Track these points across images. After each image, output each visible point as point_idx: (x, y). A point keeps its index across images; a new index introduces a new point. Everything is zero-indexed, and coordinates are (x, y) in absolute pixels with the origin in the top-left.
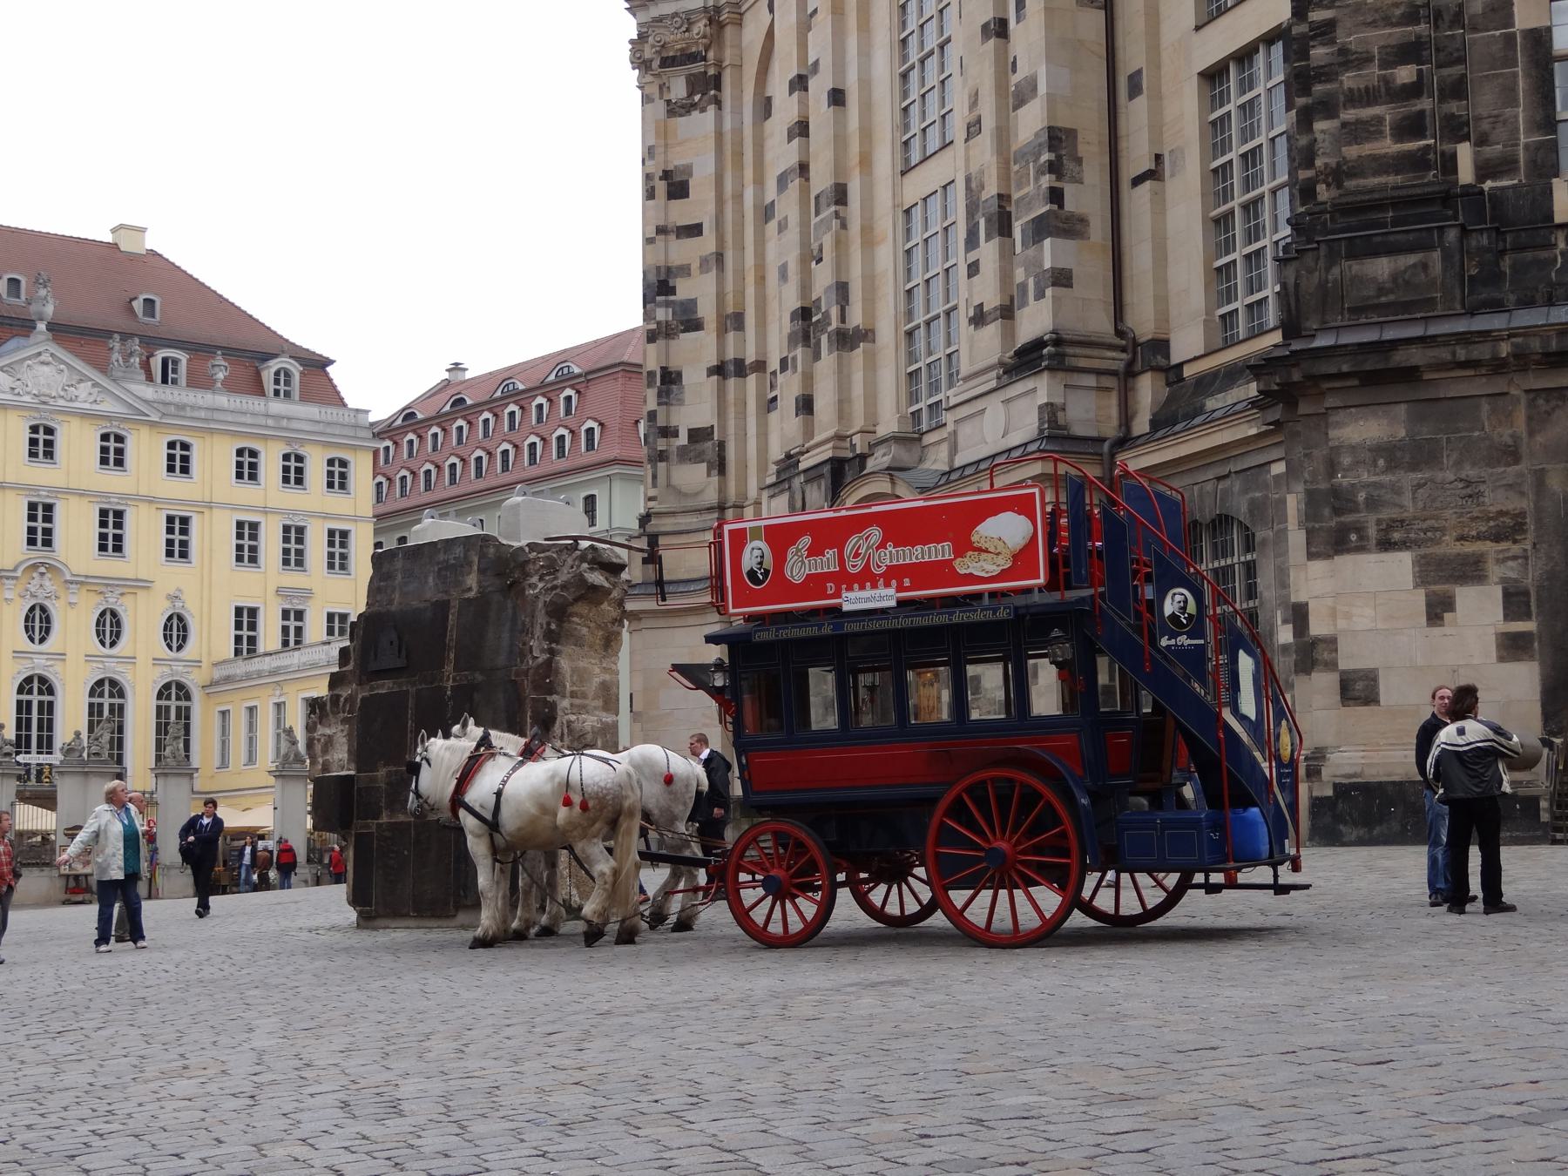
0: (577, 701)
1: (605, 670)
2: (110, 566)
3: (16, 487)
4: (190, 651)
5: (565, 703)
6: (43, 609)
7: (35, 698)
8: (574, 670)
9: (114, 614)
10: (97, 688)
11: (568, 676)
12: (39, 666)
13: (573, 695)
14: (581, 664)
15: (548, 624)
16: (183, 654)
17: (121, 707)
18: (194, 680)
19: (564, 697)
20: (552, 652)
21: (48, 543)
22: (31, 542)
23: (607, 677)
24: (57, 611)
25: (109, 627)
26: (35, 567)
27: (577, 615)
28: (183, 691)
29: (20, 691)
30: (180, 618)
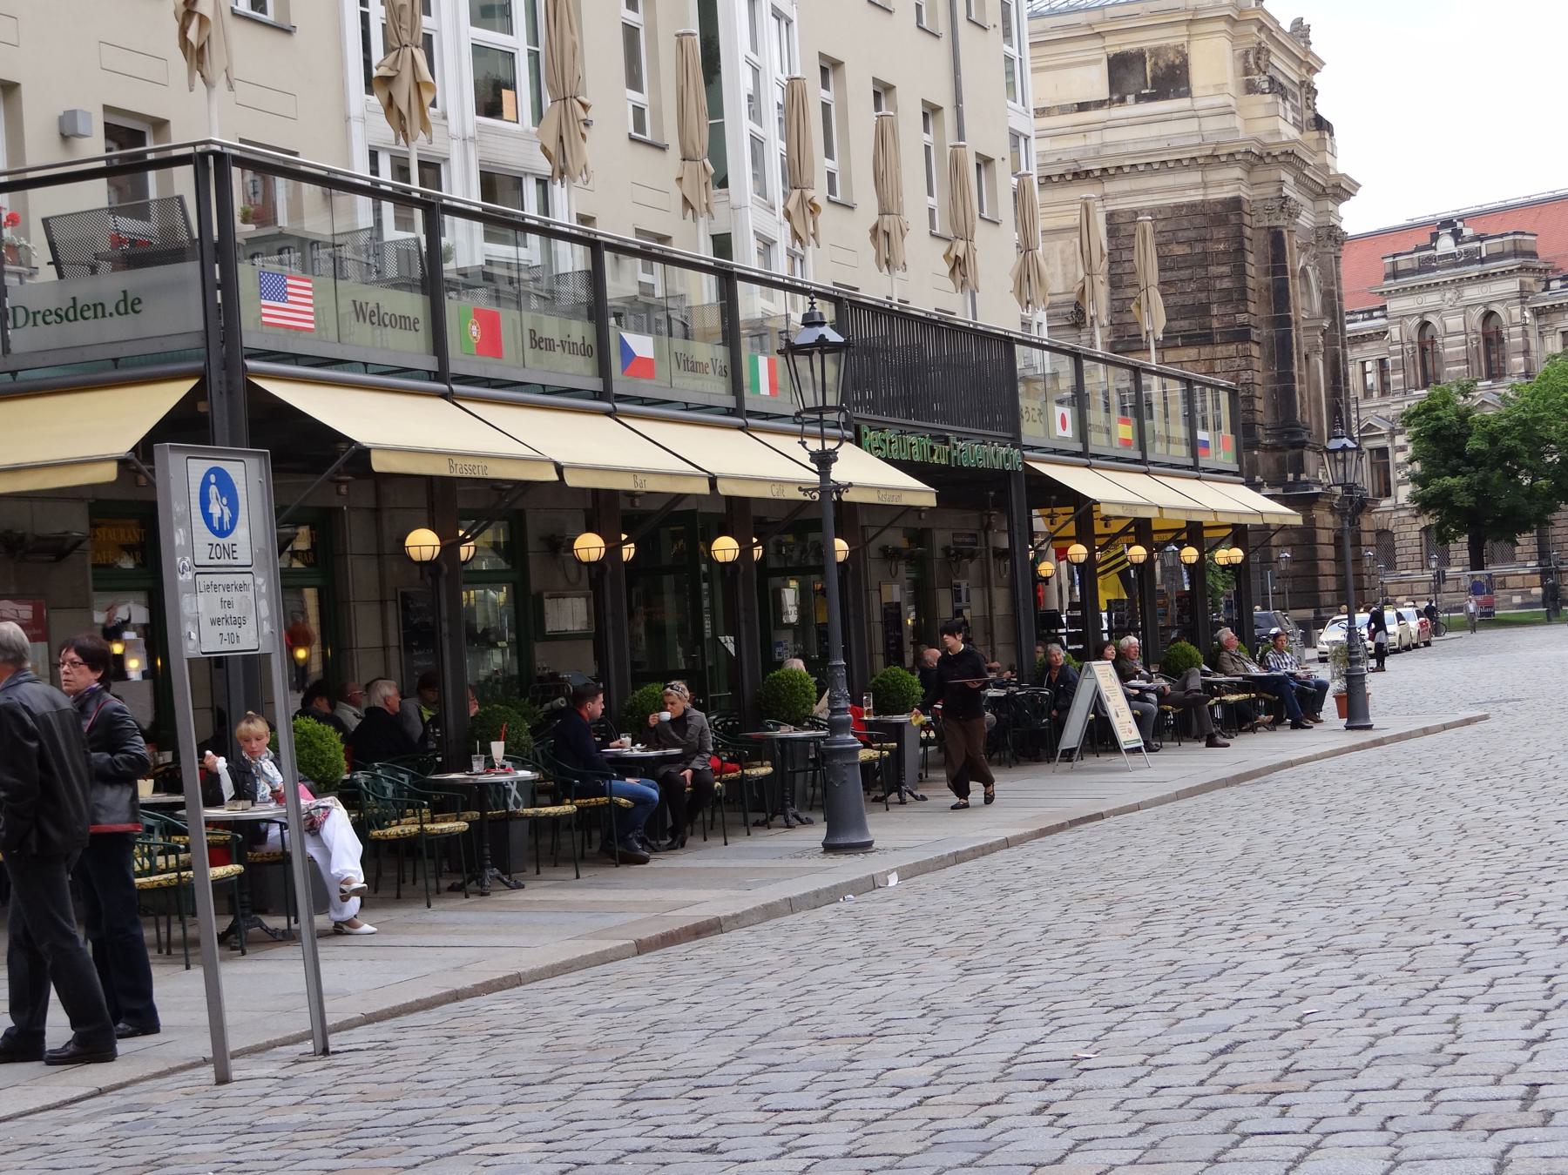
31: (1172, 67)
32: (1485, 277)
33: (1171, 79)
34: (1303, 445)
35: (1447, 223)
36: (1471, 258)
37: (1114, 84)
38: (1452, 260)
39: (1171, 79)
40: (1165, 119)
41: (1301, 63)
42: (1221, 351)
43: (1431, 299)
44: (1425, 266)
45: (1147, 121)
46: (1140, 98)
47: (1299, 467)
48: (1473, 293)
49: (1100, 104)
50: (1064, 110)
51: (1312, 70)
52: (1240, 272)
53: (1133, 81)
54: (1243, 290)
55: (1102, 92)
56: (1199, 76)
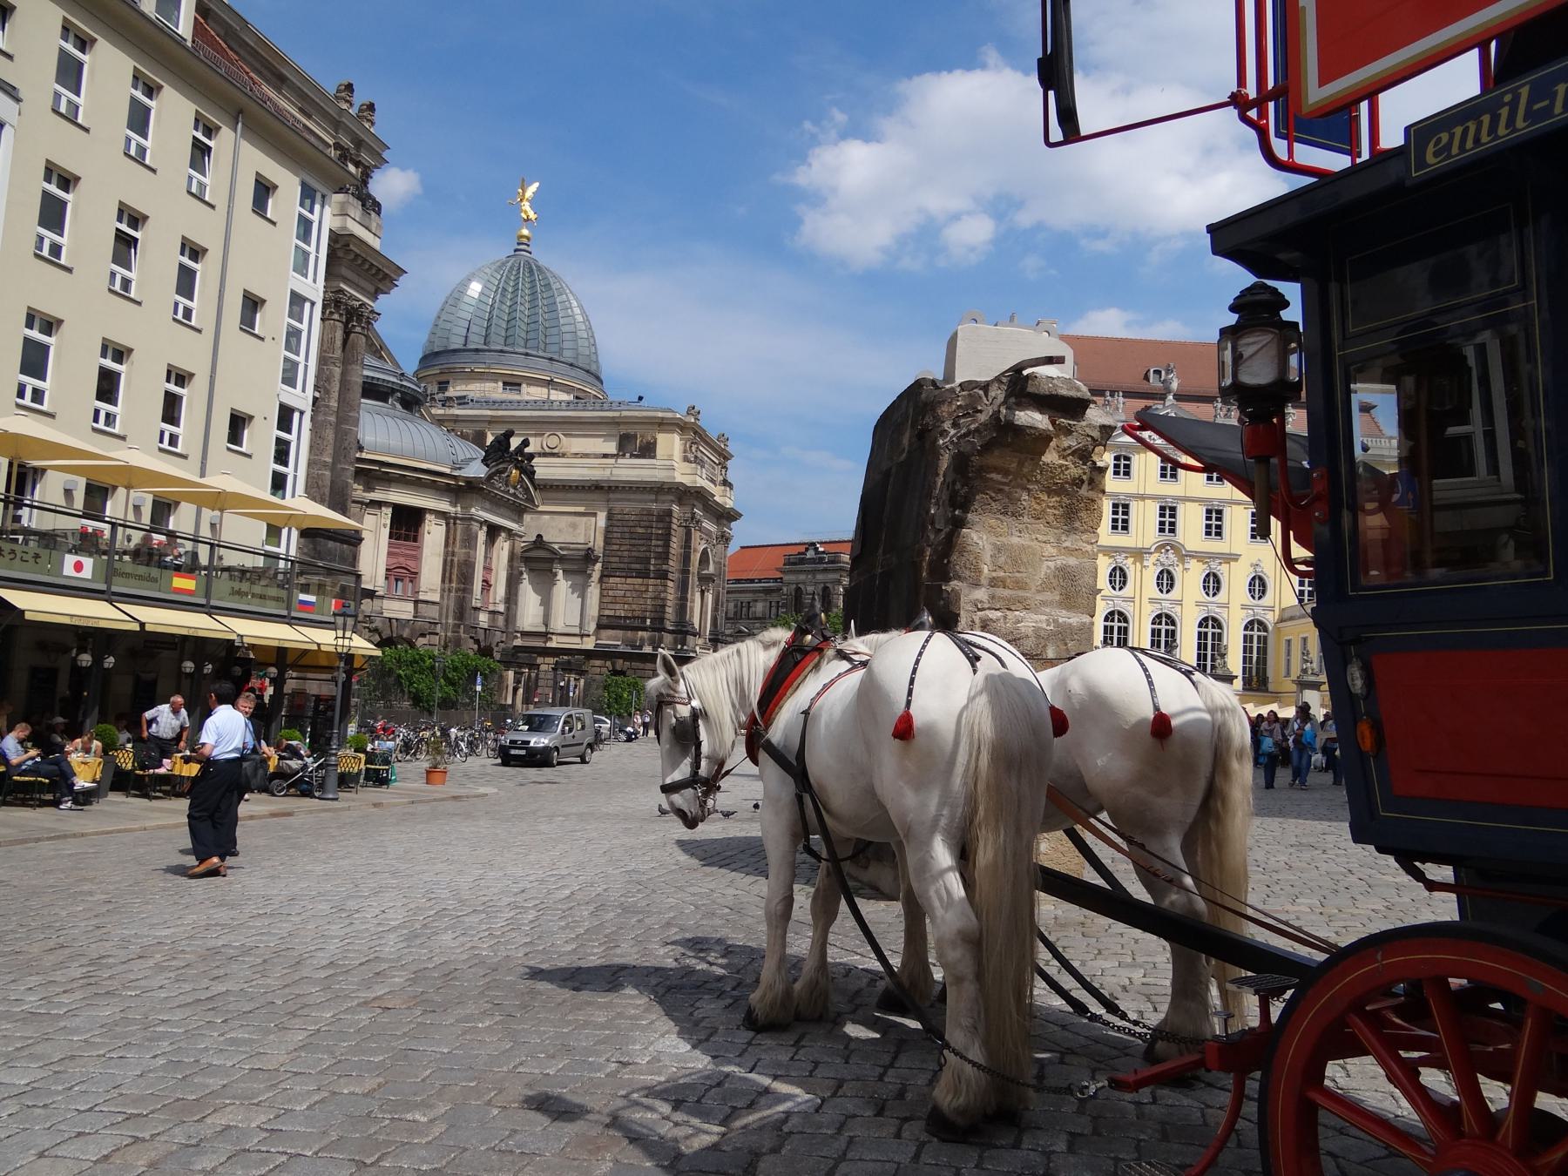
0: (1000, 592)
1: (1071, 551)
2: (1214, 546)
3: (1153, 498)
4: (1267, 600)
5: (981, 594)
6: (1169, 572)
7: (1163, 627)
8: (999, 549)
9: (1215, 576)
10: (1203, 623)
11: (987, 558)
12: (1166, 608)
13: (994, 583)
14: (1015, 540)
15: (954, 483)
16: (1261, 602)
17: (1126, 629)
18: (1270, 618)
19: (976, 585)
20: (959, 523)
21: (1172, 531)
22: (1162, 530)
23: (1072, 561)
24: (1177, 572)
25: (1213, 583)
26: (1163, 546)
27: (996, 470)
28: (1262, 625)
29: (1200, 625)
30: (1261, 579)
31: (649, 443)
32: (825, 570)
33: (648, 451)
34: (687, 633)
35: (813, 544)
36: (821, 560)
37: (621, 447)
38: (812, 561)
39: (648, 451)
40: (642, 467)
41: (720, 454)
42: (651, 581)
43: (802, 577)
44: (802, 561)
45: (633, 467)
46: (632, 456)
47: (684, 644)
48: (820, 577)
49: (612, 456)
50: (596, 456)
51: (726, 459)
52: (667, 546)
53: (630, 447)
54: (668, 553)
55: (614, 452)
56: (660, 450)
